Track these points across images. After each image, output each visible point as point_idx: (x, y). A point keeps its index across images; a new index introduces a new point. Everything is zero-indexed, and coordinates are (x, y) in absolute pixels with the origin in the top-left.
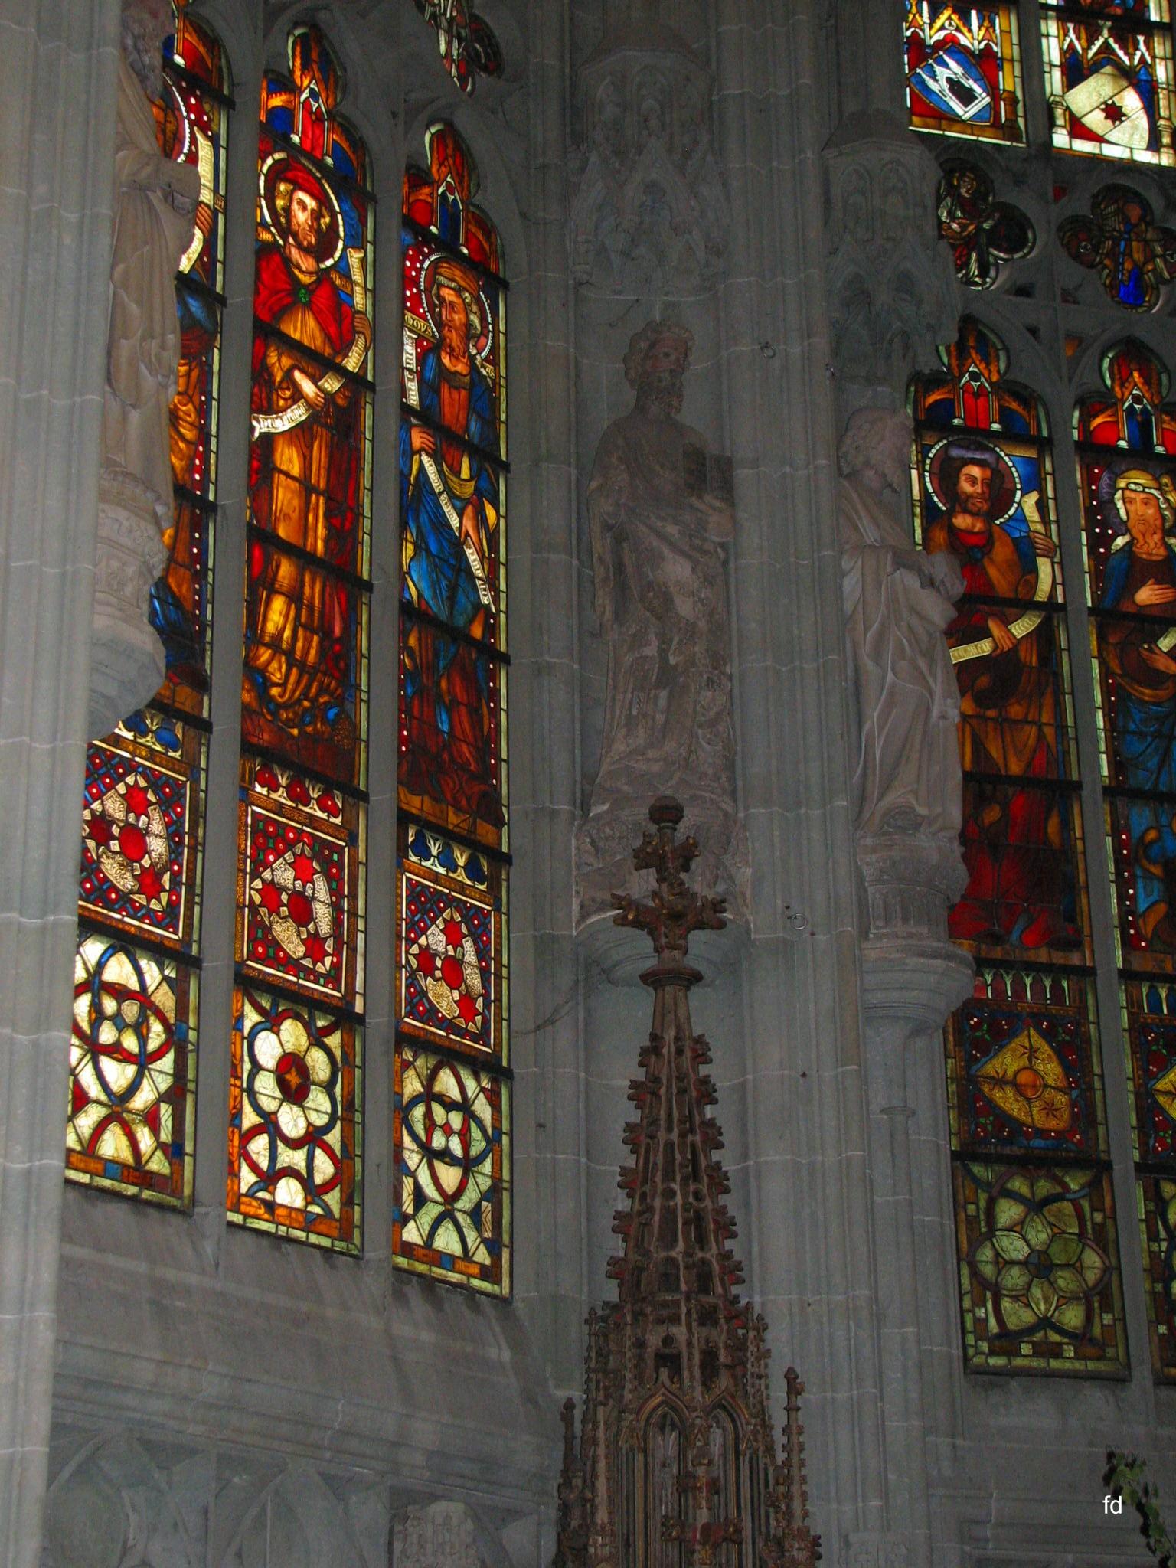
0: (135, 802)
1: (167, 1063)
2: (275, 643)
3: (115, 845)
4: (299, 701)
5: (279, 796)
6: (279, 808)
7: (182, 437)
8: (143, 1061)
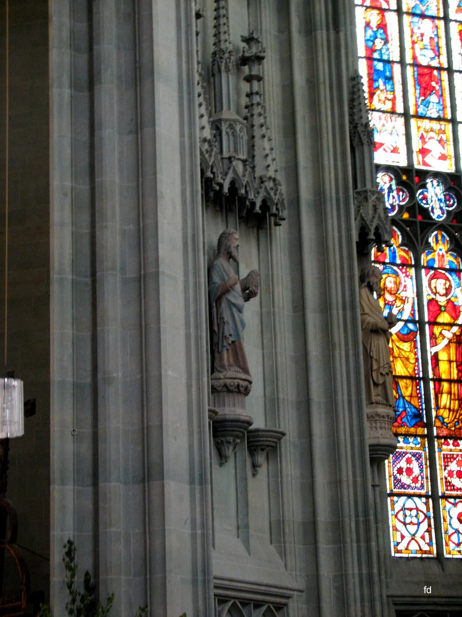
0: (409, 461)
1: (425, 523)
2: (445, 408)
3: (404, 473)
4: (453, 420)
5: (451, 447)
6: (451, 450)
7: (411, 363)
8: (419, 524)
